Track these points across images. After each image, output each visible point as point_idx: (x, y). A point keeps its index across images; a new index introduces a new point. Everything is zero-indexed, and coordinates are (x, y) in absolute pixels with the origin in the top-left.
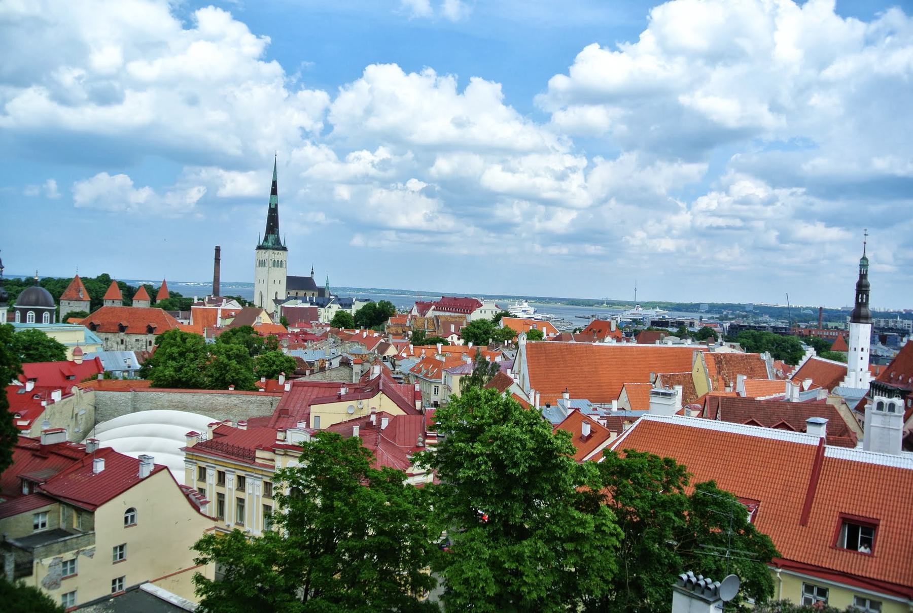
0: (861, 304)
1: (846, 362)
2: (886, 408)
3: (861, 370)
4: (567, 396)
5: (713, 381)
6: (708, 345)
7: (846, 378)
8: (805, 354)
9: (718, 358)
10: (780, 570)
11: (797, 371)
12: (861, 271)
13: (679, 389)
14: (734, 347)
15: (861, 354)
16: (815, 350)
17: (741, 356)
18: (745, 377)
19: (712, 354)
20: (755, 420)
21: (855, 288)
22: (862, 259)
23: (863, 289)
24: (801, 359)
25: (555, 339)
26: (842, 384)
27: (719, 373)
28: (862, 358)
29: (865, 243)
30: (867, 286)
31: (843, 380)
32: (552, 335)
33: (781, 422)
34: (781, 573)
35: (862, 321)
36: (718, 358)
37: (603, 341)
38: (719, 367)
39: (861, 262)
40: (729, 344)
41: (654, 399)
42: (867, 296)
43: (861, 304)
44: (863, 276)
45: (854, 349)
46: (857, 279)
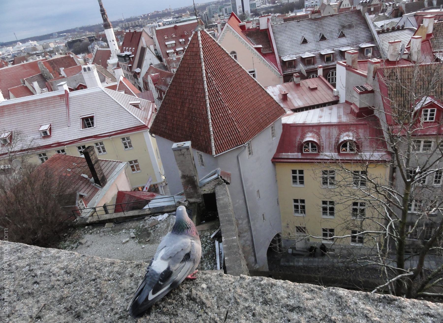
0: (105, 20)
2: (87, 70)
5: (53, 74)
7: (111, 55)
13: (36, 84)
14: (61, 54)
15: (113, 43)
17: (61, 58)
18: (63, 68)
19: (47, 61)
21: (100, 12)
27: (54, 70)
31: (111, 57)
38: (53, 67)
43: (105, 20)
44: (101, 6)
46: (99, 8)
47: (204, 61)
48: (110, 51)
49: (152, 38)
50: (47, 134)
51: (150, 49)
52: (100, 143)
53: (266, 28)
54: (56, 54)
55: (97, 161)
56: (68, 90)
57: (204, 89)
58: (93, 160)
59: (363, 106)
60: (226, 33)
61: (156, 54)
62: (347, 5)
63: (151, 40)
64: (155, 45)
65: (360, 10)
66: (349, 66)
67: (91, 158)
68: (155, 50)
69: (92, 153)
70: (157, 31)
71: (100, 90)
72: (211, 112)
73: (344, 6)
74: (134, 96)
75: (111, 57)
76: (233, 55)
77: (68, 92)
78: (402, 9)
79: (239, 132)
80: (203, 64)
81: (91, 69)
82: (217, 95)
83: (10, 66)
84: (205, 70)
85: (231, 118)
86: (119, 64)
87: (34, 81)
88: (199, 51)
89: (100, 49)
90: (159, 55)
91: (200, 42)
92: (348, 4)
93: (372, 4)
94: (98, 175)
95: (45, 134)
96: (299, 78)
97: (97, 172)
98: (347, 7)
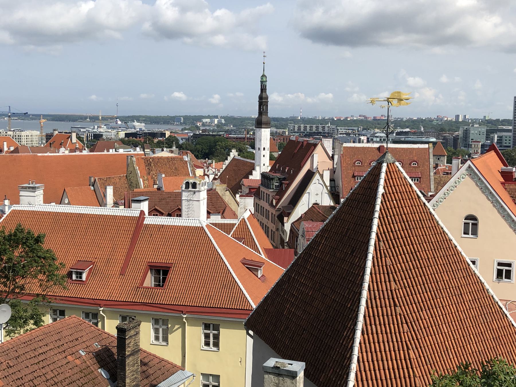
1: (254, 160)
3: (264, 165)
4: (7, 202)
5: (144, 181)
6: (144, 151)
7: (254, 172)
8: (229, 155)
9: (147, 161)
10: (102, 309)
11: (224, 169)
12: (261, 86)
14: (172, 152)
16: (237, 151)
19: (142, 158)
20: (156, 207)
22: (262, 76)
23: (263, 101)
24: (227, 159)
25: (12, 152)
26: (251, 177)
28: (264, 156)
29: (264, 63)
30: (267, 98)
31: (252, 175)
32: (12, 149)
33: (178, 208)
34: (103, 311)
35: (263, 126)
36: (147, 161)
37: (58, 153)
38: (148, 168)
39: (261, 79)
40: (169, 149)
41: (22, 193)
42: (267, 106)
44: (263, 89)
45: (258, 149)
48: (254, 164)
49: (332, 158)
50: (81, 278)
51: (322, 176)
52: (163, 320)
54: (163, 150)
55: (137, 351)
56: (146, 212)
58: (129, 347)
60: (463, 178)
61: (331, 187)
64: (334, 172)
67: (127, 342)
68: (332, 180)
69: (132, 332)
71: (199, 225)
72: (365, 317)
74: (260, 253)
75: (252, 175)
76: (471, 222)
77: (145, 215)
79: (415, 376)
81: (197, 186)
83: (85, 152)
84: (377, 234)
85: (406, 342)
86: (261, 189)
87: (109, 185)
89: (239, 158)
94: (128, 381)
95: (77, 277)
97: (128, 372)
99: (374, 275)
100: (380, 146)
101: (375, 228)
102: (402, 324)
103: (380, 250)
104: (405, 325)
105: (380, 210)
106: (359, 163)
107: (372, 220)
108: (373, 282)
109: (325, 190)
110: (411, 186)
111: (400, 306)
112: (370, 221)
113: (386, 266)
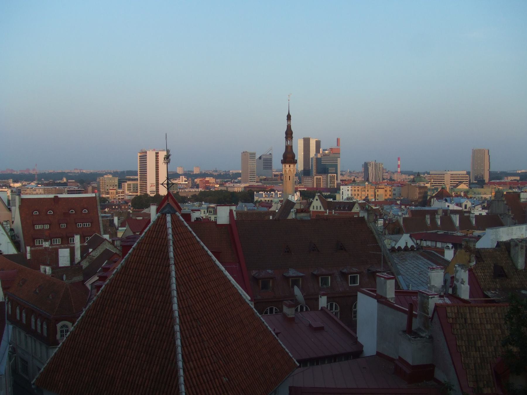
47: (175, 264)
49: (10, 210)
53: (228, 223)
57: (172, 311)
59: (417, 363)
61: (12, 236)
62: (319, 208)
63: (7, 212)
64: (13, 222)
65: (364, 217)
66: (382, 297)
70: (22, 200)
73: (315, 208)
78: (399, 224)
80: (173, 267)
82: (193, 325)
84: (176, 279)
85: (217, 370)
88: (167, 246)
90: (17, 239)
91: (170, 231)
92: (320, 207)
93: (353, 211)
96: (293, 309)
98: (319, 210)
99: (181, 317)
100: (55, 196)
101: (173, 273)
102: (211, 355)
103: (181, 293)
104: (213, 356)
105: (174, 256)
106: (37, 213)
107: (169, 266)
108: (182, 323)
109: (9, 240)
110: (191, 232)
111: (207, 340)
112: (167, 267)
113: (189, 306)
